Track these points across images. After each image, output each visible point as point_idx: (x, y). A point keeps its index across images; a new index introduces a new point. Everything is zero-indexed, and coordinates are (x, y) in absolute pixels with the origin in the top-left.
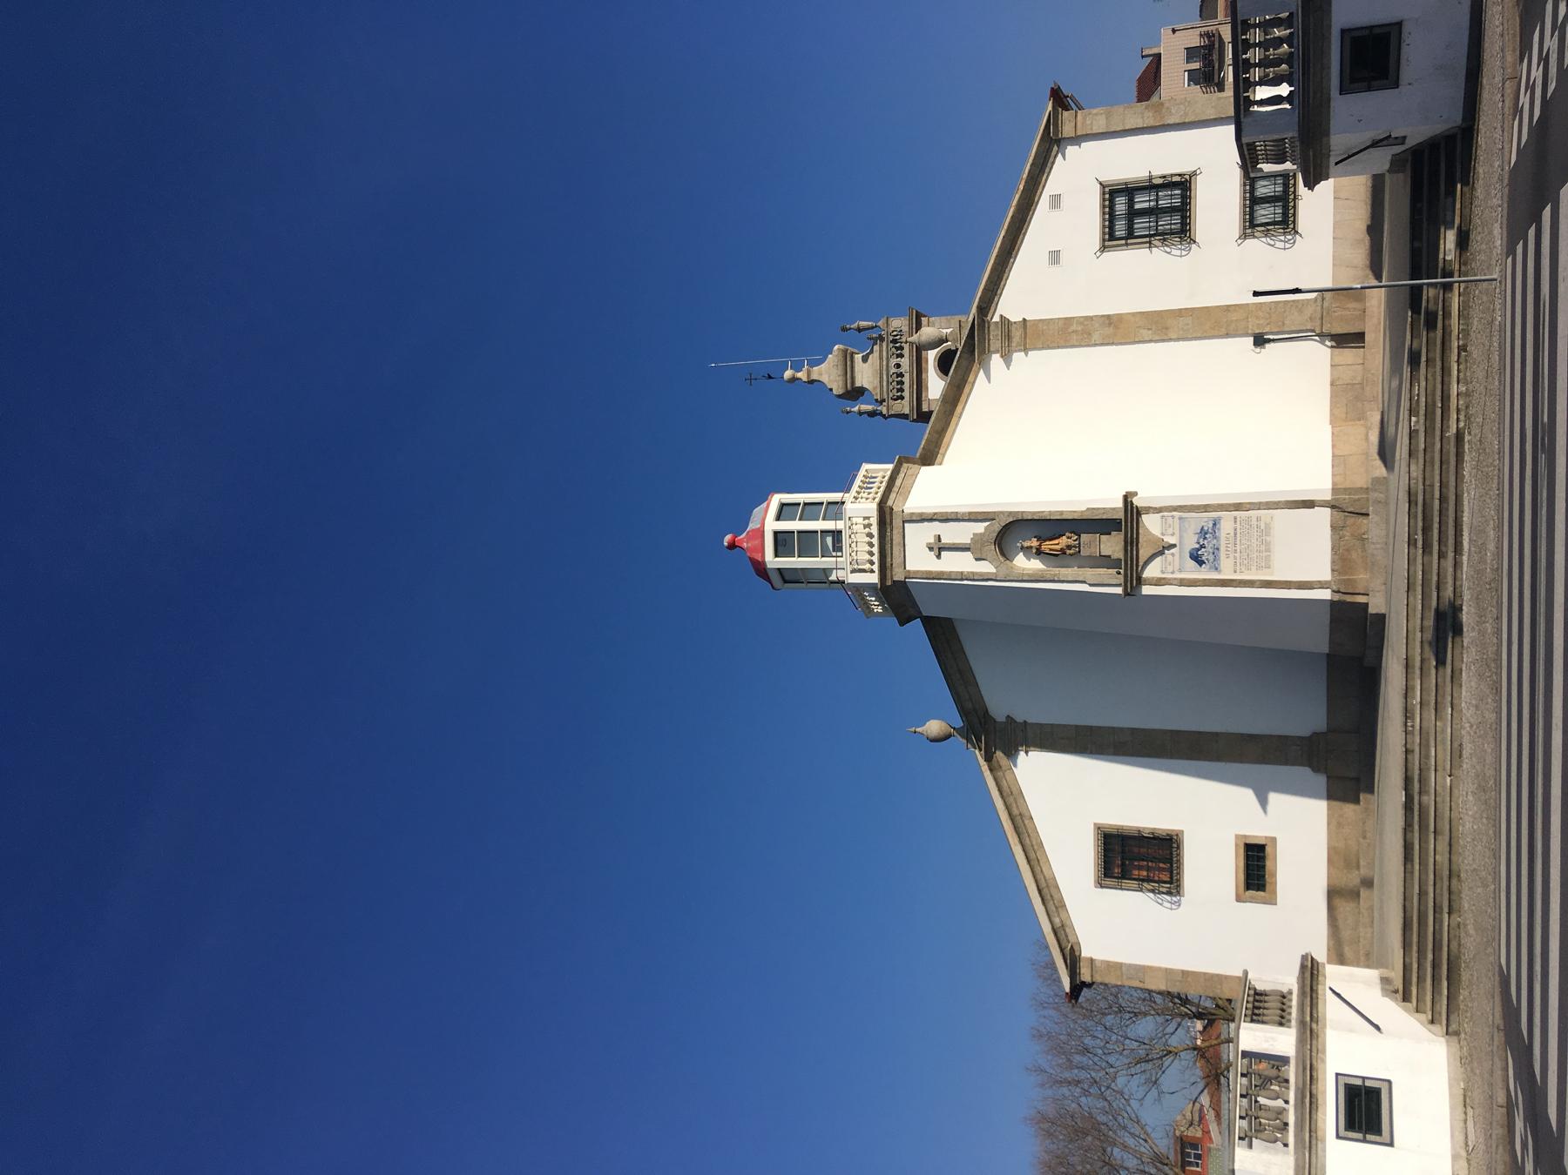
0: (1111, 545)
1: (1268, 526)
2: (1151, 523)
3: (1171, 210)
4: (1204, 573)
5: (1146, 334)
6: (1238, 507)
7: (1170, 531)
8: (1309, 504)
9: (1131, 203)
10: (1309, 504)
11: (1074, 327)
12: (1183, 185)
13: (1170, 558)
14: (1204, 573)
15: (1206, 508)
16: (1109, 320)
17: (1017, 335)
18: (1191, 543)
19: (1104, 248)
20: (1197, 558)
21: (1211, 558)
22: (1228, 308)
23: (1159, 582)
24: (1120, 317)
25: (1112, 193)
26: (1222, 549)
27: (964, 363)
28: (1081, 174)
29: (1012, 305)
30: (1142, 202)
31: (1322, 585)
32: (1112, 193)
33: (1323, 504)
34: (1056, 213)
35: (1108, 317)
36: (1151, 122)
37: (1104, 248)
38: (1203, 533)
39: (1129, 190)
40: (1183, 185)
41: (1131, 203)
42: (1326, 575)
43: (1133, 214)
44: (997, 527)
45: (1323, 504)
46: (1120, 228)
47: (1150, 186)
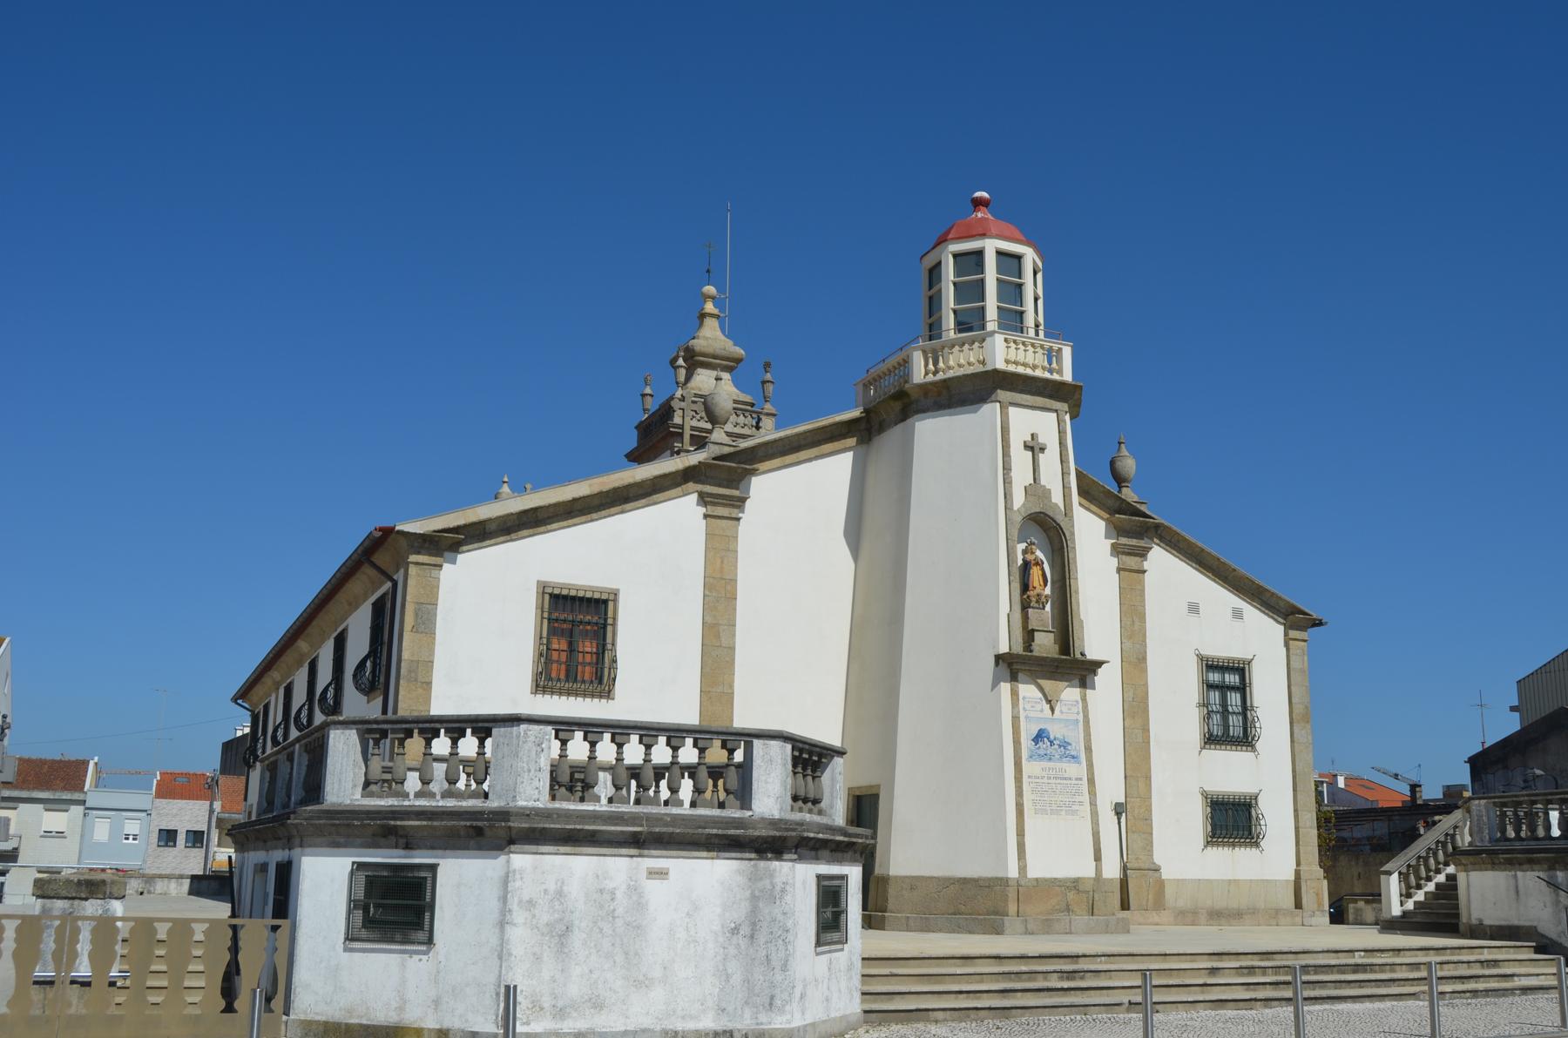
0: (1045, 644)
1: (1074, 812)
2: (1070, 694)
3: (1226, 726)
4: (1026, 743)
5: (1130, 694)
6: (1091, 781)
7: (1065, 709)
8: (1098, 858)
9: (1233, 688)
10: (1098, 858)
11: (1137, 623)
12: (1245, 740)
13: (1038, 707)
14: (1026, 743)
15: (1089, 749)
16: (1142, 659)
17: (1131, 562)
18: (1055, 731)
19: (1201, 658)
20: (1039, 737)
21: (1042, 752)
22: (1148, 778)
23: (1015, 694)
24: (1145, 670)
25: (1240, 669)
26: (1051, 764)
27: (1110, 502)
28: (1259, 640)
29: (1160, 562)
30: (1234, 699)
31: (1023, 869)
32: (1240, 669)
33: (1098, 869)
34: (1229, 612)
35: (1144, 659)
36: (1298, 709)
37: (1201, 658)
38: (1065, 745)
39: (1243, 688)
40: (1245, 740)
41: (1233, 688)
42: (1033, 873)
43: (1223, 688)
44: (1060, 519)
45: (1098, 869)
46: (1215, 677)
47: (1245, 708)
